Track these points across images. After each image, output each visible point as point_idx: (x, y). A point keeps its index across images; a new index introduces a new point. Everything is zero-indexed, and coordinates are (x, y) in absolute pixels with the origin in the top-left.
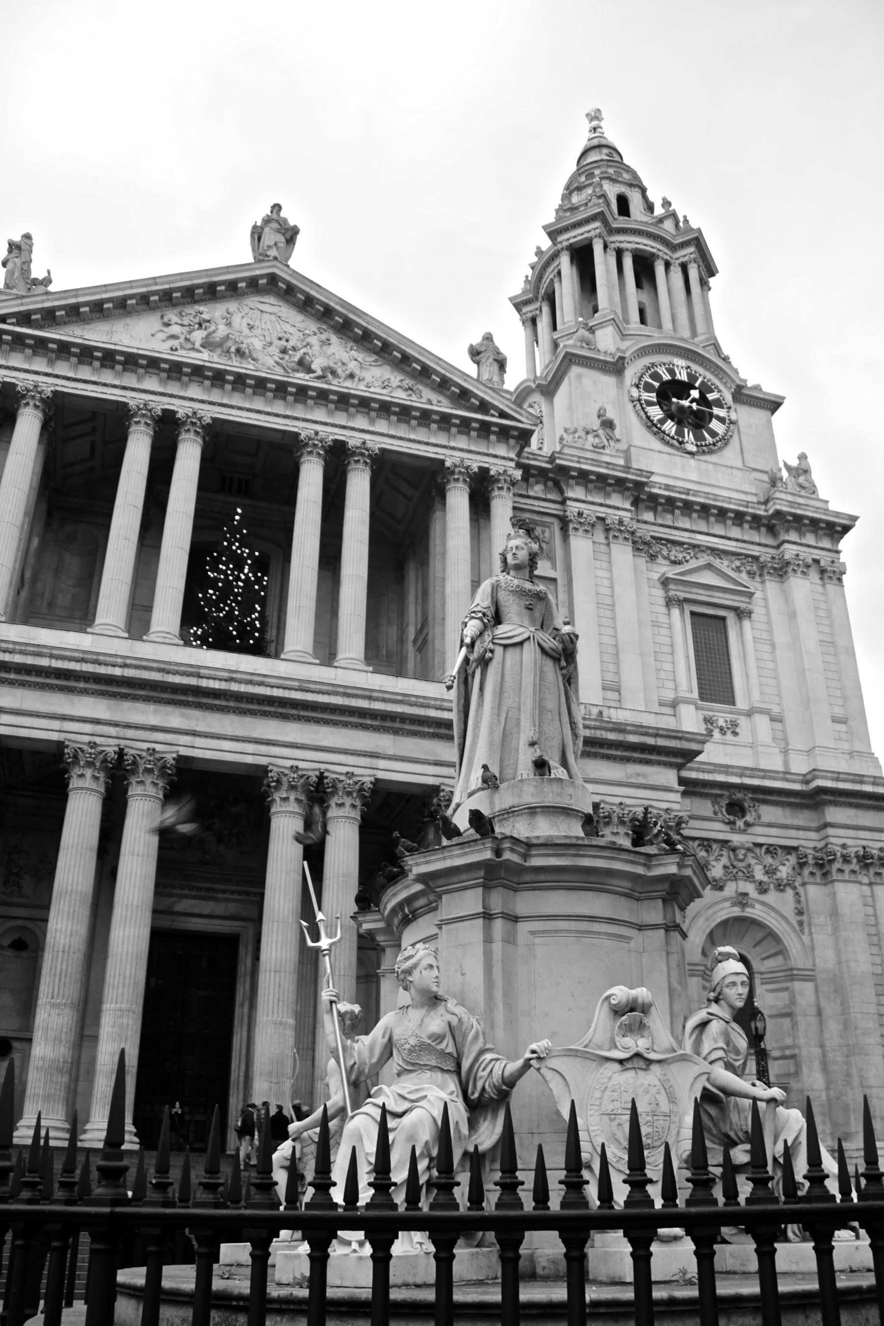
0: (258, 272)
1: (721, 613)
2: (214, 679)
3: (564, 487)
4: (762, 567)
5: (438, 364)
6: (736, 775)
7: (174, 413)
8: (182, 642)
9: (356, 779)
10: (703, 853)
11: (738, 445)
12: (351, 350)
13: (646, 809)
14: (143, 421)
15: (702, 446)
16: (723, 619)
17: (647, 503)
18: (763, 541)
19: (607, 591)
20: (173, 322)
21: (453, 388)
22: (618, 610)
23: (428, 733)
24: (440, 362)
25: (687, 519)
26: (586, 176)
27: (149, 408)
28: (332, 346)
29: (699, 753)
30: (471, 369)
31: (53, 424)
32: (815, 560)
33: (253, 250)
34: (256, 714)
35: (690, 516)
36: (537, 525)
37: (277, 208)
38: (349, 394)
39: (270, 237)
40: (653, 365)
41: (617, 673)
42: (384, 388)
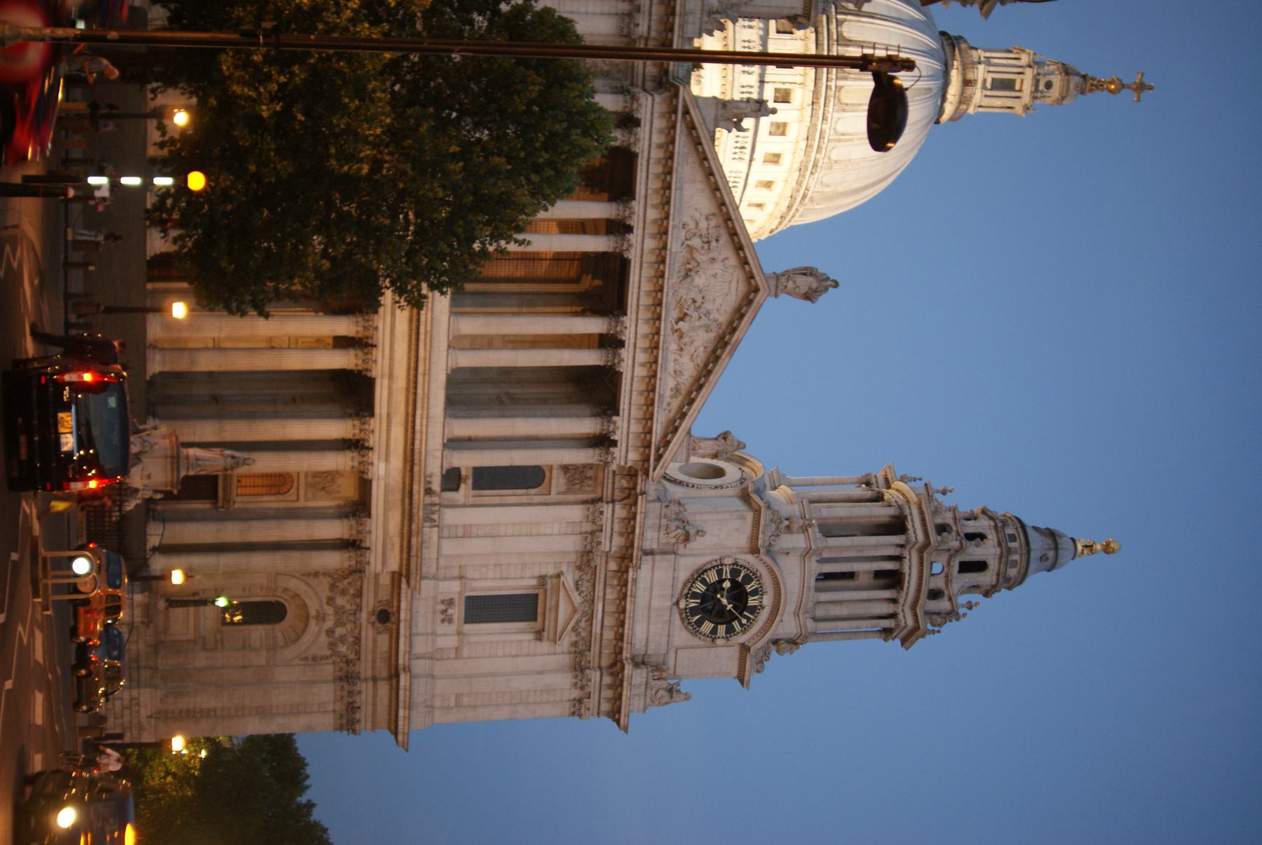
0: (758, 279)
1: (540, 618)
3: (625, 502)
4: (581, 653)
10: (352, 591)
12: (705, 347)
15: (687, 613)
16: (535, 620)
20: (710, 222)
25: (615, 596)
26: (1014, 535)
33: (794, 270)
37: (836, 284)
39: (805, 283)
40: (759, 579)
42: (675, 372)
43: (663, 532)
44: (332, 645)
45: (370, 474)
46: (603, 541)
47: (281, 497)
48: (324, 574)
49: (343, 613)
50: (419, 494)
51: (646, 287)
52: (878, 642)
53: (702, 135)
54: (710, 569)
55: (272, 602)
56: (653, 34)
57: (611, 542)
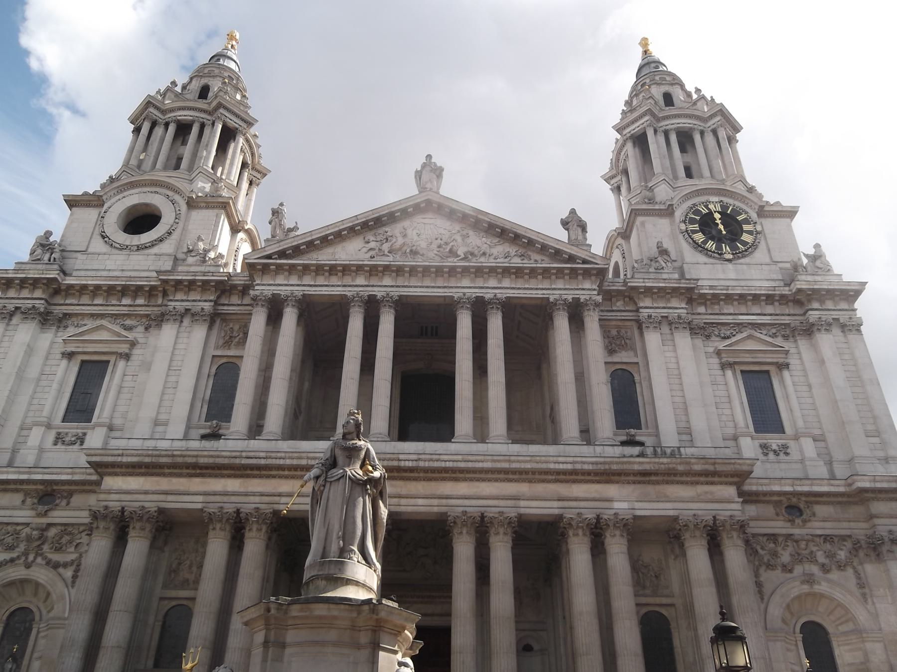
2: (409, 460)
4: (794, 330)
5: (538, 237)
6: (789, 485)
7: (375, 296)
8: (388, 439)
9: (505, 515)
10: (772, 545)
11: (765, 247)
13: (714, 517)
14: (357, 304)
15: (736, 253)
16: (767, 372)
17: (700, 301)
18: (792, 312)
19: (674, 366)
21: (550, 250)
22: (684, 377)
23: (552, 480)
24: (539, 235)
25: (730, 306)
27: (360, 295)
28: (470, 237)
29: (752, 472)
30: (562, 235)
31: (306, 314)
32: (833, 319)
33: (418, 186)
34: (438, 480)
35: (732, 305)
36: (621, 328)
37: (429, 157)
38: (483, 266)
40: (694, 205)
41: (688, 422)
42: (506, 258)
43: (662, 271)
44: (841, 567)
45: (627, 517)
46: (677, 314)
47: (673, 625)
48: (757, 575)
49: (799, 554)
50: (642, 463)
51: (427, 282)
52: (739, 147)
53: (290, 245)
54: (692, 239)
55: (803, 638)
56: (212, 298)
57: (678, 308)
